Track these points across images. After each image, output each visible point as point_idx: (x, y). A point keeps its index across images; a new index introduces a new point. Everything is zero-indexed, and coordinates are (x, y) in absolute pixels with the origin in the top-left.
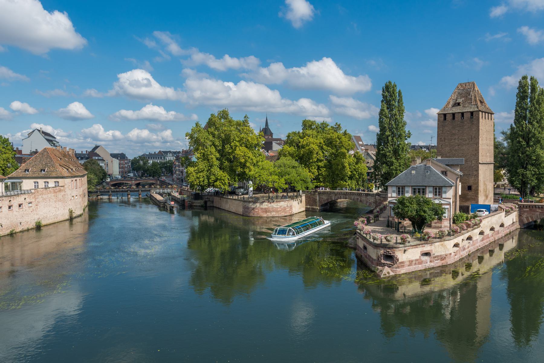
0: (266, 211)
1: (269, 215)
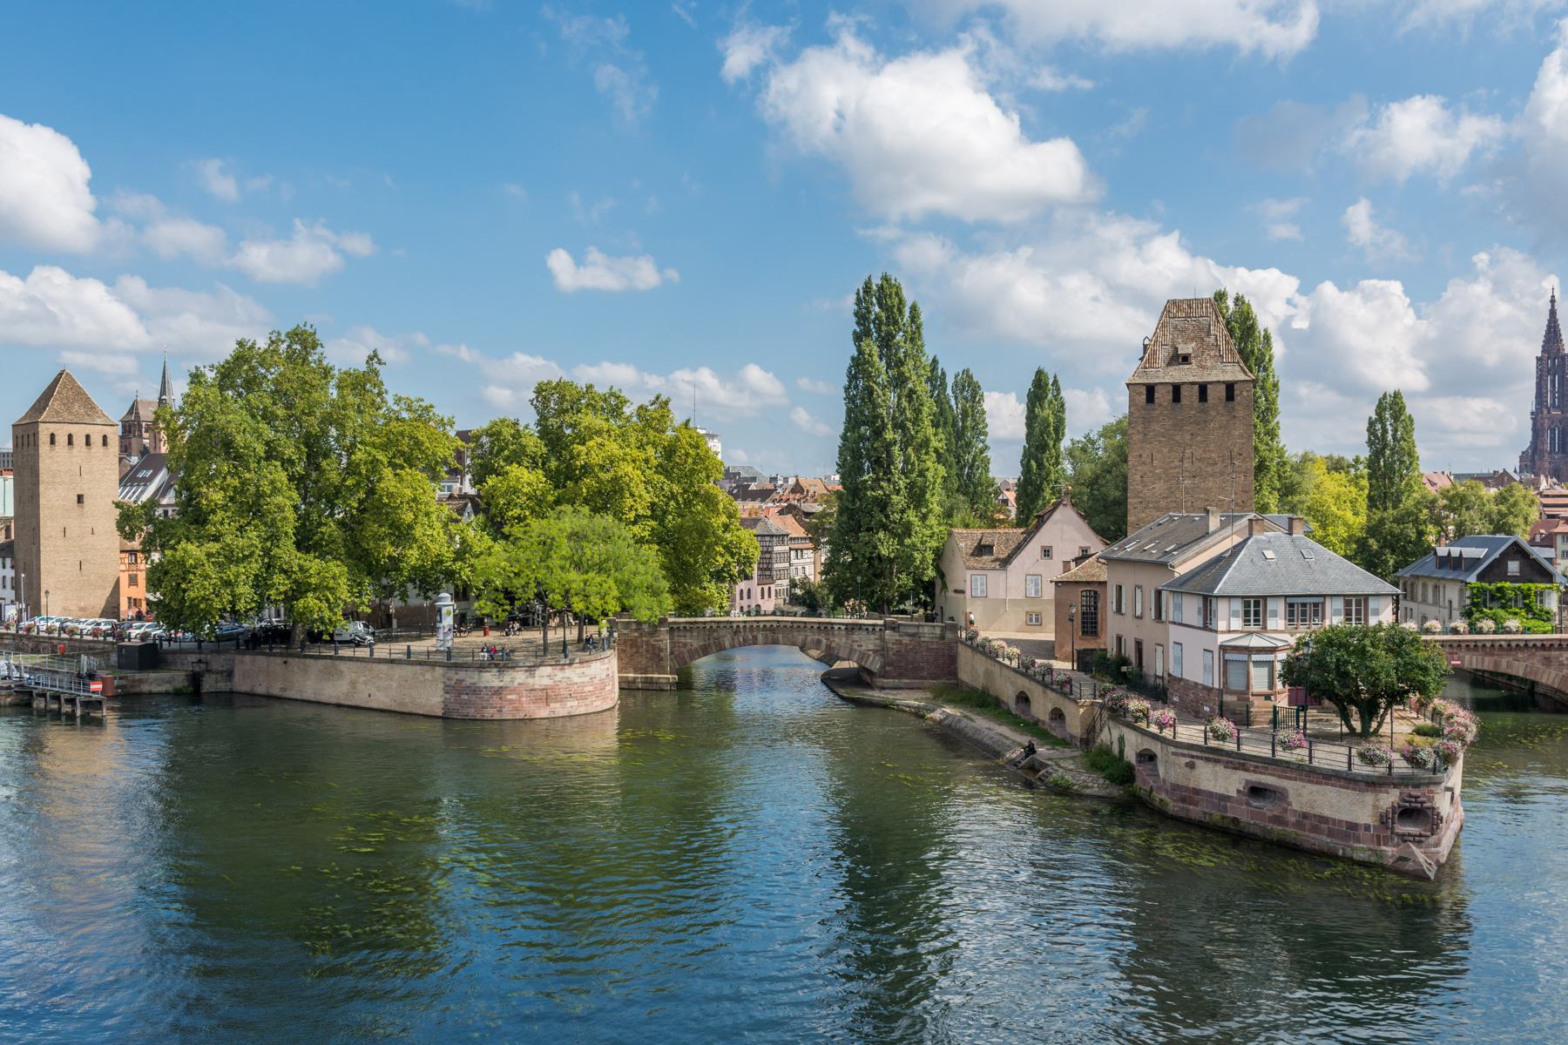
0: (547, 696)
1: (559, 709)
